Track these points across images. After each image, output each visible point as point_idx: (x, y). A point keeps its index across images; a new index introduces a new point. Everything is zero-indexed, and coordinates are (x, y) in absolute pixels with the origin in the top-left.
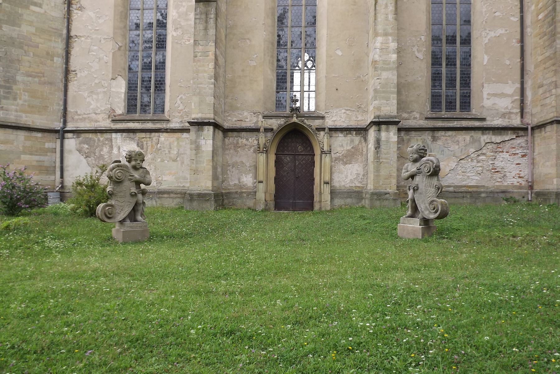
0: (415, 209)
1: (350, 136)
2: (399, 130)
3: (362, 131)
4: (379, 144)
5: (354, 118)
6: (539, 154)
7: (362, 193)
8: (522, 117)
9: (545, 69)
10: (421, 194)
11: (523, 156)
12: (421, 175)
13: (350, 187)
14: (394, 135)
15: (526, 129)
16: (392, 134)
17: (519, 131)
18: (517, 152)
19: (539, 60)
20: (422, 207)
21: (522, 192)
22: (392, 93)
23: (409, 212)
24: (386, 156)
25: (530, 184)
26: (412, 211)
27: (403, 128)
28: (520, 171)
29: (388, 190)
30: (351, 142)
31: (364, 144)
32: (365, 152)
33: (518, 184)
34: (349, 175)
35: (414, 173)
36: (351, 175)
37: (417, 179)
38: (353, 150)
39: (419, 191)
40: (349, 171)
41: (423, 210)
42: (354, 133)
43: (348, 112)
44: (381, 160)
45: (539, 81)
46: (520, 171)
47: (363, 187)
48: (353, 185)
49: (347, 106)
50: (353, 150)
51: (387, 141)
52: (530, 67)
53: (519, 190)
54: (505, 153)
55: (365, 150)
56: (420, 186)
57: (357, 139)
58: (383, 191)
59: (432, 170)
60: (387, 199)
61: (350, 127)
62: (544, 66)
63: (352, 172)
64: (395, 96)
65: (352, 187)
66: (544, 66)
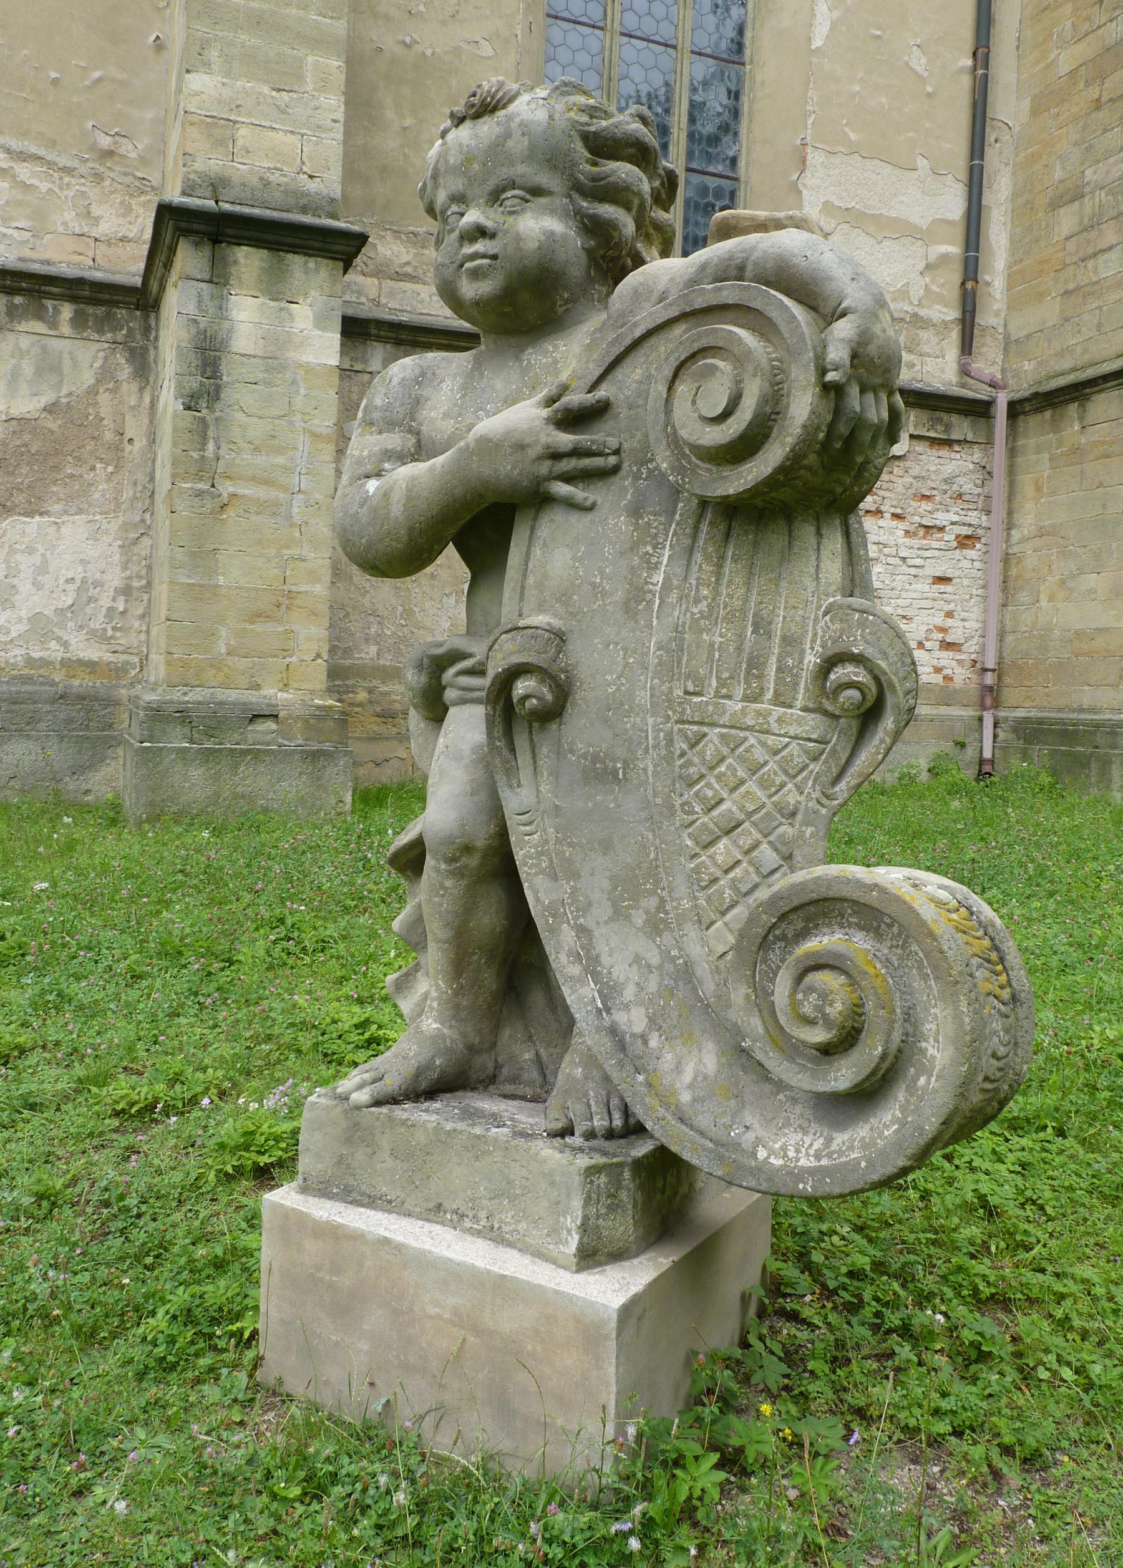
0: (510, 967)
1: (39, 327)
2: (356, 330)
3: (117, 305)
4: (215, 375)
5: (67, 217)
6: (1042, 532)
7: (111, 702)
8: (967, 346)
9: (1098, 104)
10: (602, 773)
11: (965, 541)
12: (610, 503)
13: (30, 661)
14: (320, 322)
15: (979, 410)
16: (303, 316)
17: (955, 419)
18: (941, 518)
19: (1064, 68)
20: (619, 968)
21: (951, 718)
22: (318, 42)
23: (424, 1016)
24: (261, 460)
25: (989, 679)
26: (455, 1011)
27: (379, 323)
28: (949, 614)
29: (272, 694)
30: (39, 372)
31: (129, 389)
32: (140, 443)
33: (938, 679)
34: (25, 586)
35: (507, 470)
36: (38, 586)
37: (553, 557)
38: (53, 424)
39: (581, 730)
40: (26, 562)
41: (634, 1020)
42: (67, 311)
43: (23, 171)
44: (226, 488)
45: (1058, 174)
46: (949, 614)
47: (118, 671)
48: (54, 651)
49: (24, 134)
50: (53, 424)
51: (274, 360)
52: (1009, 107)
53: (944, 710)
54: (887, 522)
55: (134, 428)
56: (603, 664)
57: (82, 356)
58: (233, 695)
59: (802, 407)
60: (257, 755)
61: (36, 268)
62: (1094, 92)
63: (42, 568)
64: (335, 64)
65: (45, 663)
66: (1094, 92)
